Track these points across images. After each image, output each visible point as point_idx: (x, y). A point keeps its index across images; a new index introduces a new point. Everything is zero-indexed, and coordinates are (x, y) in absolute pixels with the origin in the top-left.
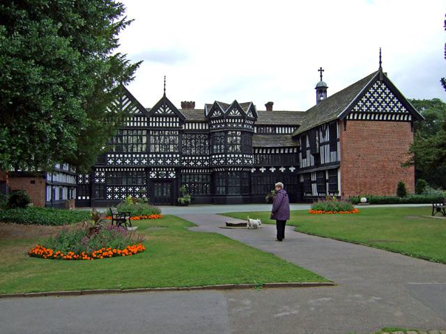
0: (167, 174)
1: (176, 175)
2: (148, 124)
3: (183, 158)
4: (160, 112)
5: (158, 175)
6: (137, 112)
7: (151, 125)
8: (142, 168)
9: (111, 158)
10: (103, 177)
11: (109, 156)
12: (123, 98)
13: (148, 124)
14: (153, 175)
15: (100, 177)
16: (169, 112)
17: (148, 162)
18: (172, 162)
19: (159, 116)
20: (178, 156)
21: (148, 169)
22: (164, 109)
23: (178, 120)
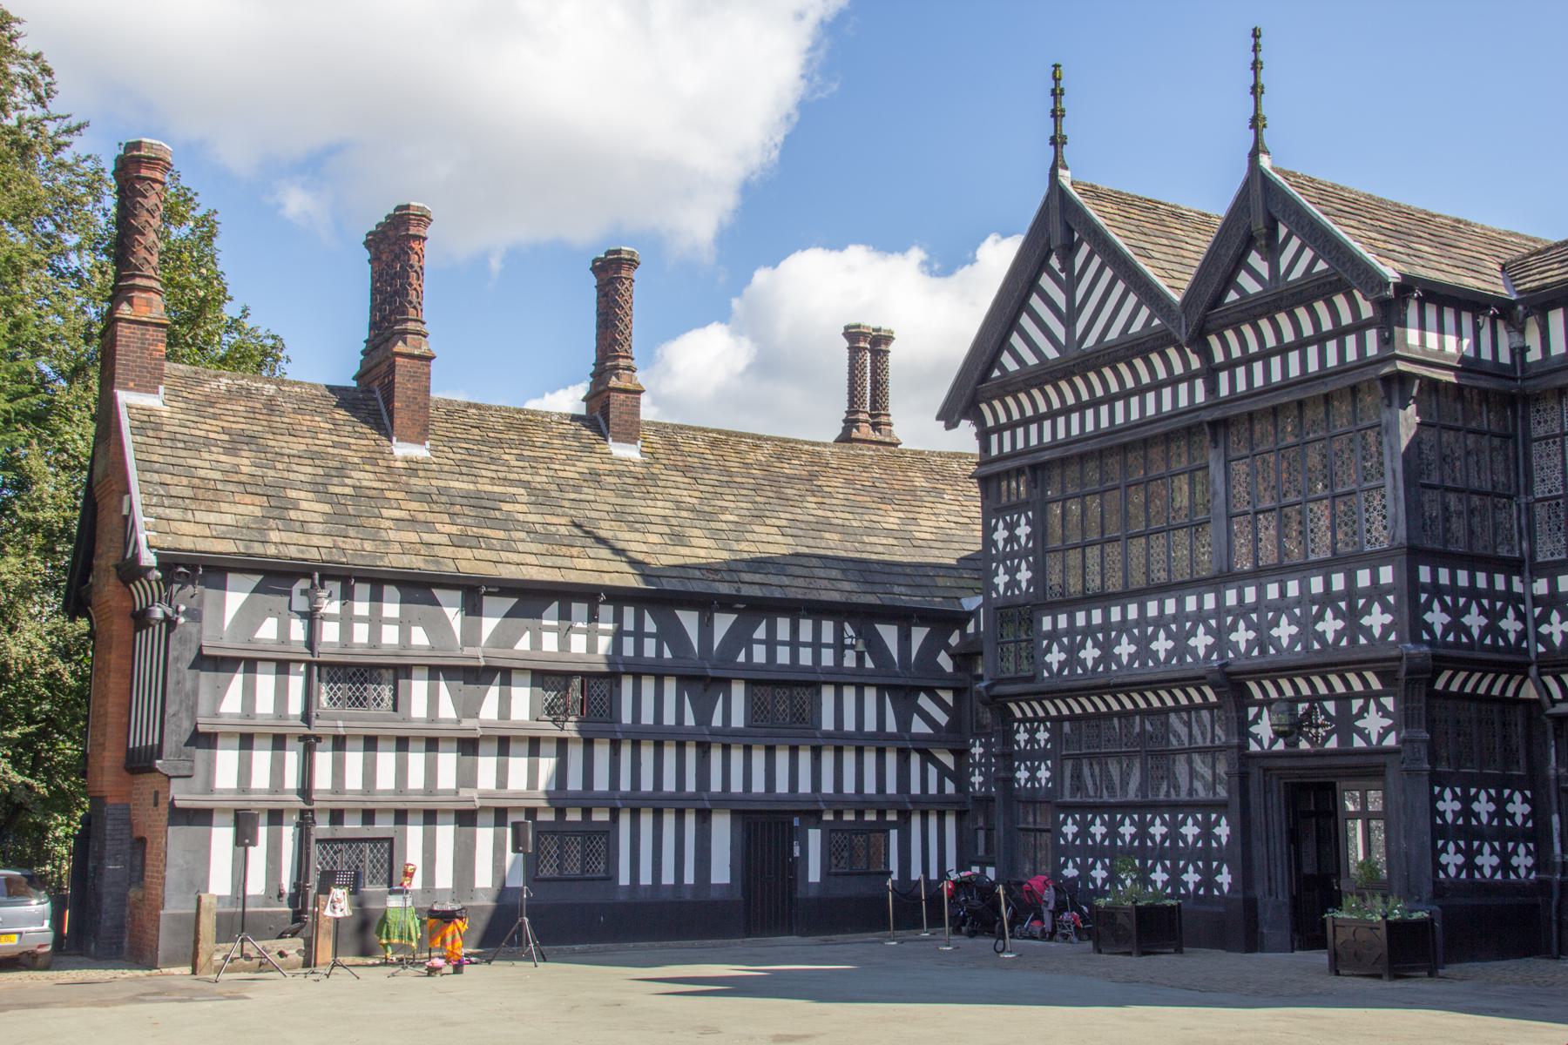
0: (1345, 724)
1: (1404, 719)
2: (1212, 388)
3: (1541, 587)
4: (1252, 287)
5: (1290, 731)
6: (1136, 327)
7: (1224, 391)
8: (1197, 681)
9: (1054, 635)
10: (1043, 755)
11: (1047, 623)
12: (1079, 261)
13: (1212, 388)
14: (1264, 729)
15: (1033, 756)
16: (1297, 273)
17: (1221, 636)
18: (1352, 617)
19: (1253, 311)
20: (1386, 575)
21: (1232, 685)
22: (1272, 251)
23: (1367, 311)
